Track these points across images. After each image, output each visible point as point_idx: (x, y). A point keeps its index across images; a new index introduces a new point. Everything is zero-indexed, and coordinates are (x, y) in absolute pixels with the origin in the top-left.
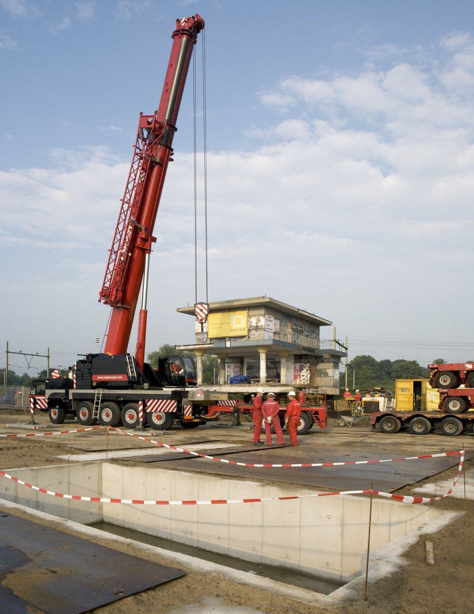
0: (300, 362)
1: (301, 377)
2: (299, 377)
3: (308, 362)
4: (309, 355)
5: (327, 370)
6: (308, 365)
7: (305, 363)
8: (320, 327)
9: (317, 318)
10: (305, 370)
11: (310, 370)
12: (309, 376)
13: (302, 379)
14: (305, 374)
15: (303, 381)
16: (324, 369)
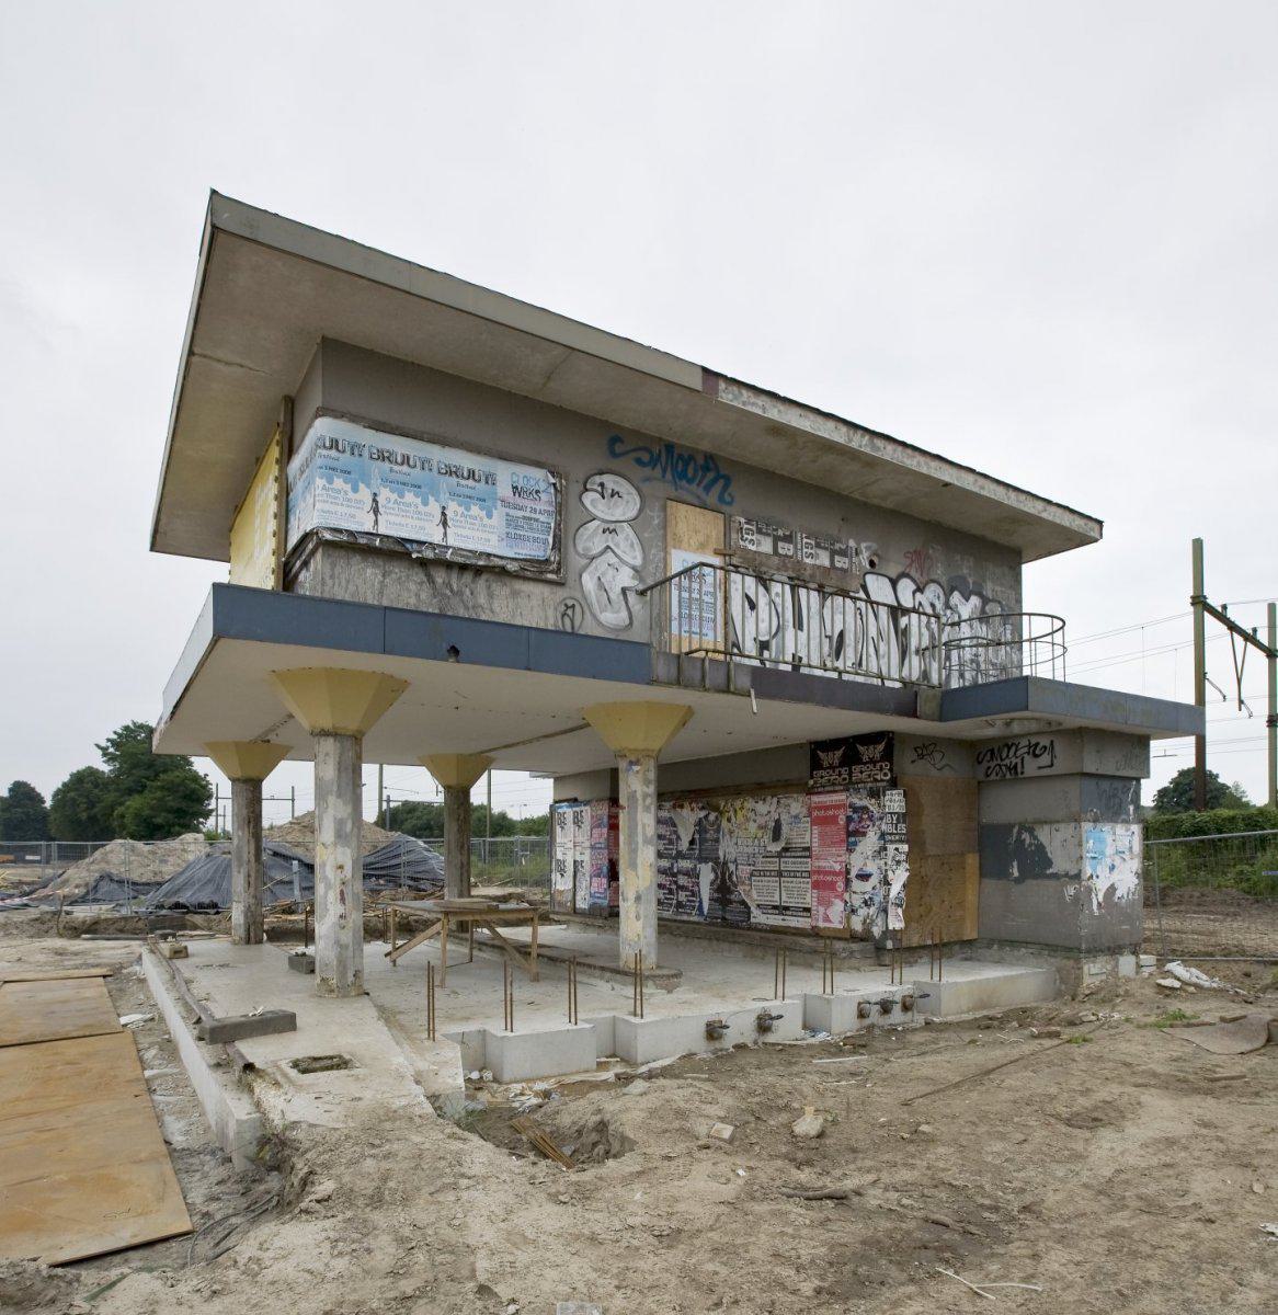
0: (849, 786)
1: (857, 885)
2: (840, 885)
3: (894, 784)
4: (907, 737)
5: (1043, 834)
6: (895, 801)
7: (875, 794)
8: (1030, 571)
9: (947, 475)
10: (870, 841)
11: (915, 840)
12: (899, 877)
13: (857, 901)
14: (871, 867)
15: (863, 912)
16: (1023, 827)
